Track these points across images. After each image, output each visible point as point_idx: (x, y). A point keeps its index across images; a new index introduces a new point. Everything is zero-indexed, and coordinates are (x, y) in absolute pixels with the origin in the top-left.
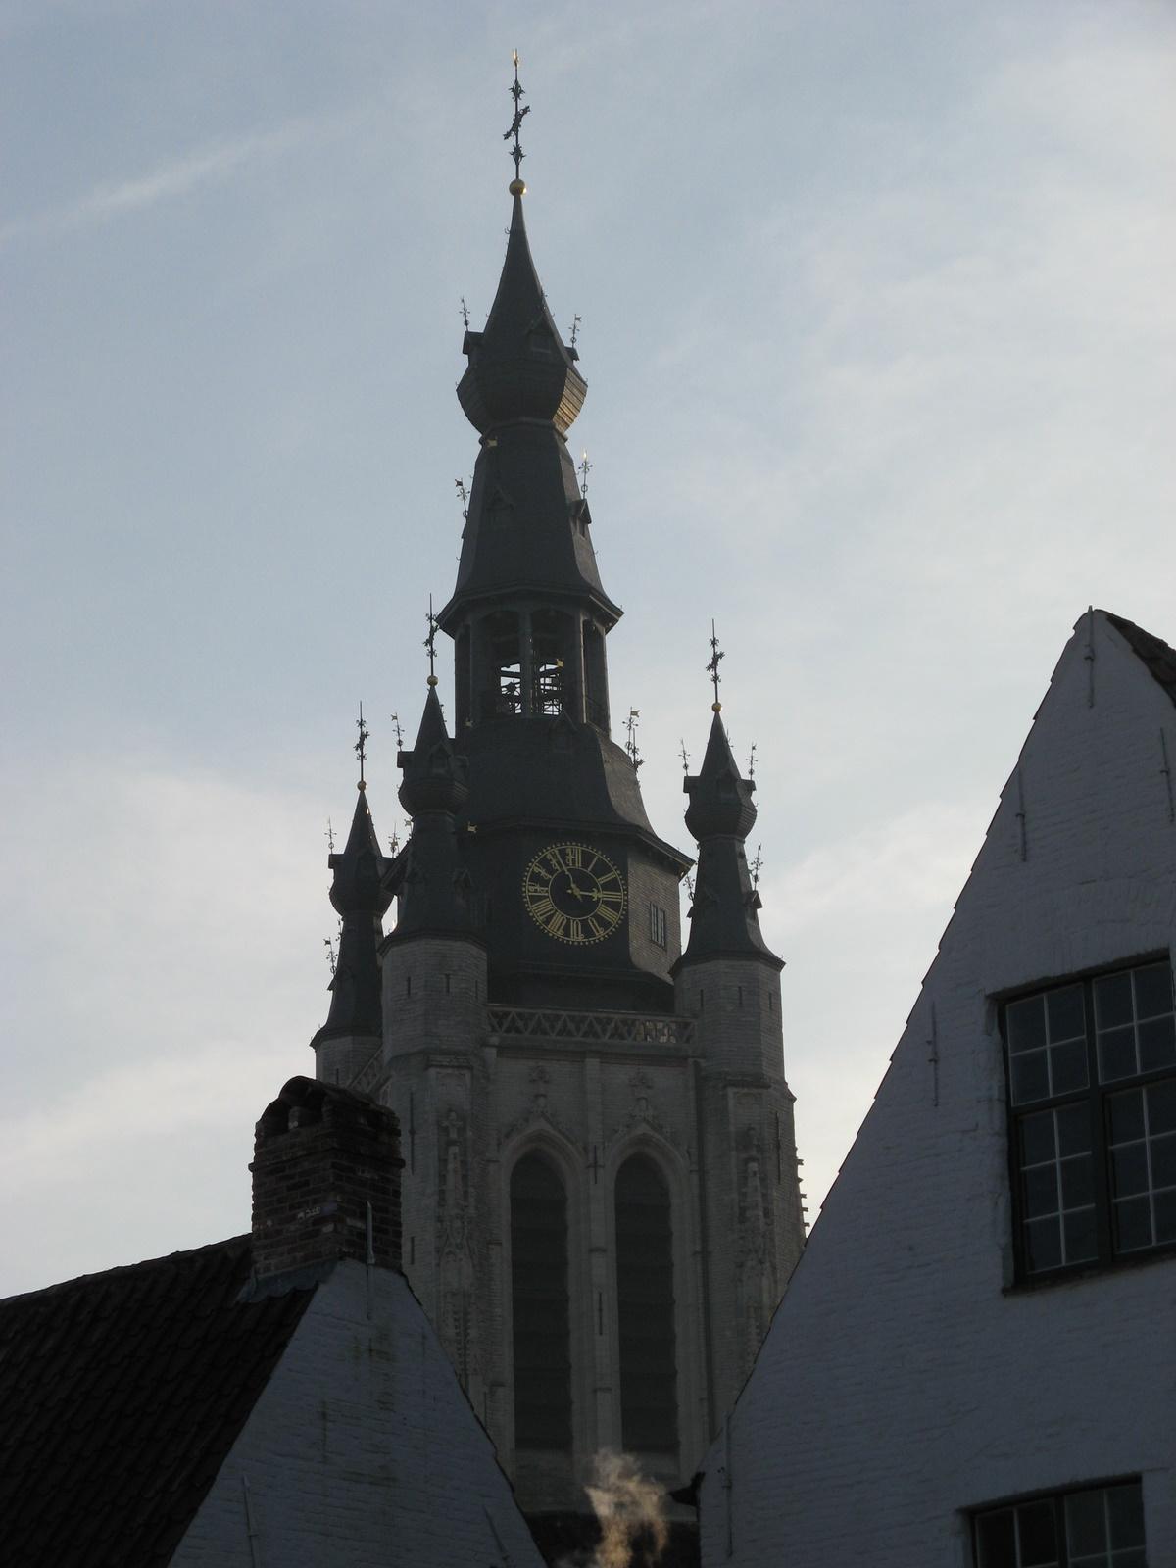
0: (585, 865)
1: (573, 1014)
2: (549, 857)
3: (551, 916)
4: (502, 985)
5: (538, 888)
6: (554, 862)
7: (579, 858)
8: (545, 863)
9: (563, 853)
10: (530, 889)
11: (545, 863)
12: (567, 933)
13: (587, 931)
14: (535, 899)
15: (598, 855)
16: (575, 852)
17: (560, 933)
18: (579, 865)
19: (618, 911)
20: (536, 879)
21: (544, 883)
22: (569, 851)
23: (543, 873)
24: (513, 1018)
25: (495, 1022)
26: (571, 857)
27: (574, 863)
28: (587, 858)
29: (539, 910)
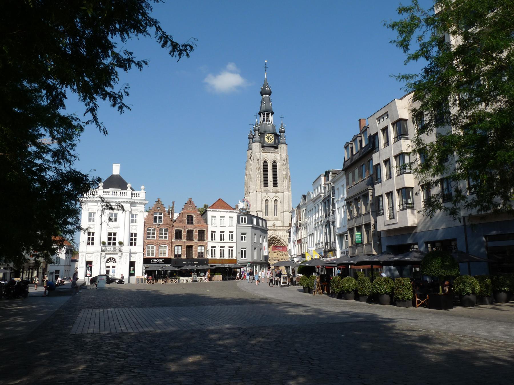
4: (263, 147)
16: (269, 135)
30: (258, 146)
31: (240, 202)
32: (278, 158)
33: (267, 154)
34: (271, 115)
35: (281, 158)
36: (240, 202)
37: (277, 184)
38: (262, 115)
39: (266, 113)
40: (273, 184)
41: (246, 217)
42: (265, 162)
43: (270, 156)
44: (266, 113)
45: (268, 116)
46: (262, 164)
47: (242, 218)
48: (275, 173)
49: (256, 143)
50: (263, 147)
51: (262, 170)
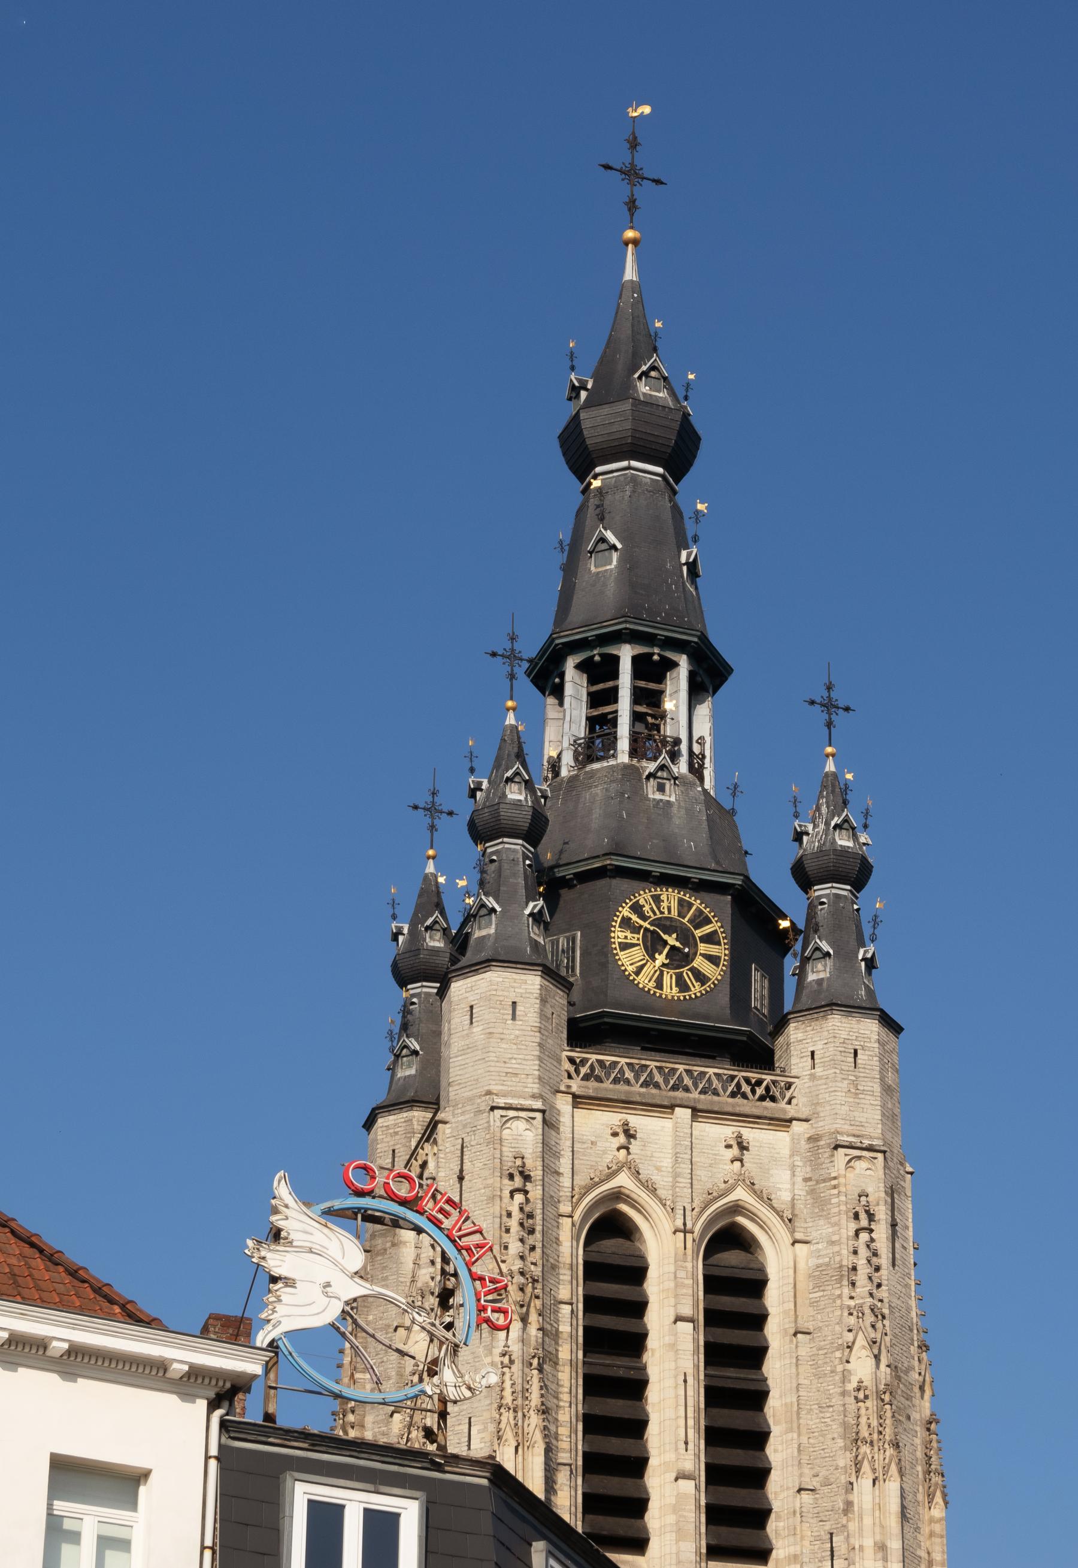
0: (681, 914)
1: (663, 1064)
2: (642, 902)
3: (643, 966)
4: (584, 1032)
5: (629, 935)
6: (647, 908)
7: (674, 905)
8: (637, 909)
9: (657, 899)
10: (619, 935)
11: (637, 909)
12: (659, 985)
13: (682, 986)
14: (625, 946)
15: (697, 904)
16: (670, 898)
17: (652, 984)
18: (674, 913)
19: (718, 966)
20: (626, 923)
21: (635, 929)
22: (664, 897)
23: (634, 918)
24: (592, 1065)
25: (572, 1069)
26: (665, 904)
27: (669, 912)
28: (684, 906)
29: (628, 960)
30: (530, 1011)
31: (297, 1220)
32: (784, 1185)
33: (638, 1121)
34: (697, 690)
35: (818, 1184)
36: (297, 1220)
37: (760, 1516)
38: (575, 683)
39: (626, 654)
40: (715, 1515)
41: (410, 1514)
42: (611, 1226)
43: (672, 1158)
44: (626, 654)
45: (648, 699)
46: (570, 1249)
47: (326, 1521)
48: (733, 1376)
49: (494, 979)
50: (584, 1032)
51: (569, 1323)
